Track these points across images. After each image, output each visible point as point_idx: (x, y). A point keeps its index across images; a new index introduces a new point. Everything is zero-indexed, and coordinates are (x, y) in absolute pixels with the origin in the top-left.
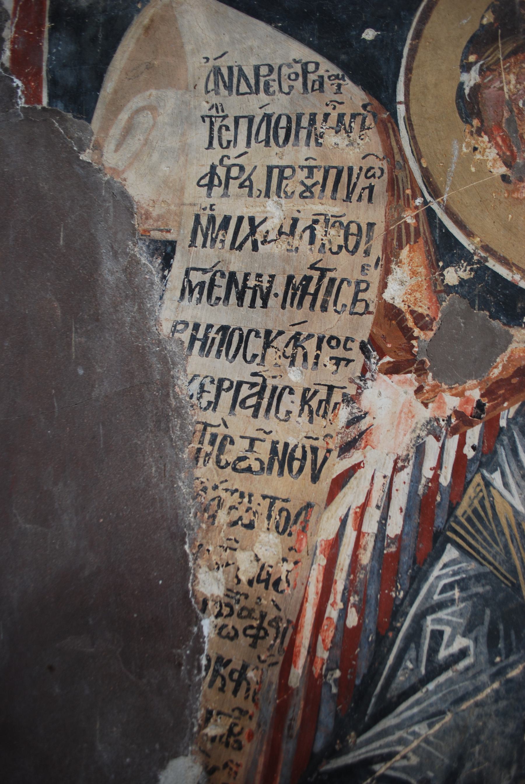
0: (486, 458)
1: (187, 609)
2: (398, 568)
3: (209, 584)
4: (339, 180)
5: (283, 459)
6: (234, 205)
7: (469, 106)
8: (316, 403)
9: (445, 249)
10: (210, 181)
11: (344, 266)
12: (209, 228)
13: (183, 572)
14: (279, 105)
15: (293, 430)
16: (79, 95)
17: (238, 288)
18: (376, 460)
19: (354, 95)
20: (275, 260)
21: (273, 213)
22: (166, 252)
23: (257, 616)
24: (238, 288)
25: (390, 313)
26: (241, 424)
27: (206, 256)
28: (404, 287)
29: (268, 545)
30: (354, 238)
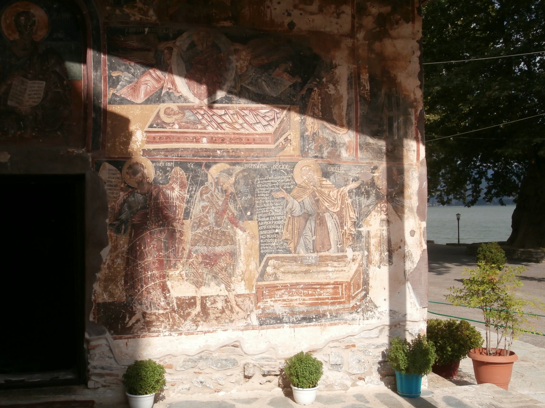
0: (128, 197)
1: (108, 208)
2: (122, 205)
3: (109, 206)
4: (118, 178)
5: (114, 197)
6: (110, 180)
7: (127, 173)
8: (117, 194)
9: (125, 183)
10: (109, 178)
11: (118, 184)
12: (109, 181)
13: (107, 205)
14: (114, 172)
15: (115, 195)
16: (98, 170)
17: (111, 186)
18: (121, 198)
19: (119, 172)
20: (114, 184)
21: (113, 180)
22: (105, 183)
23: (113, 208)
24: (111, 186)
25: (122, 188)
26: (111, 195)
27: (108, 183)
28: (122, 186)
29: (113, 203)
30: (119, 182)
